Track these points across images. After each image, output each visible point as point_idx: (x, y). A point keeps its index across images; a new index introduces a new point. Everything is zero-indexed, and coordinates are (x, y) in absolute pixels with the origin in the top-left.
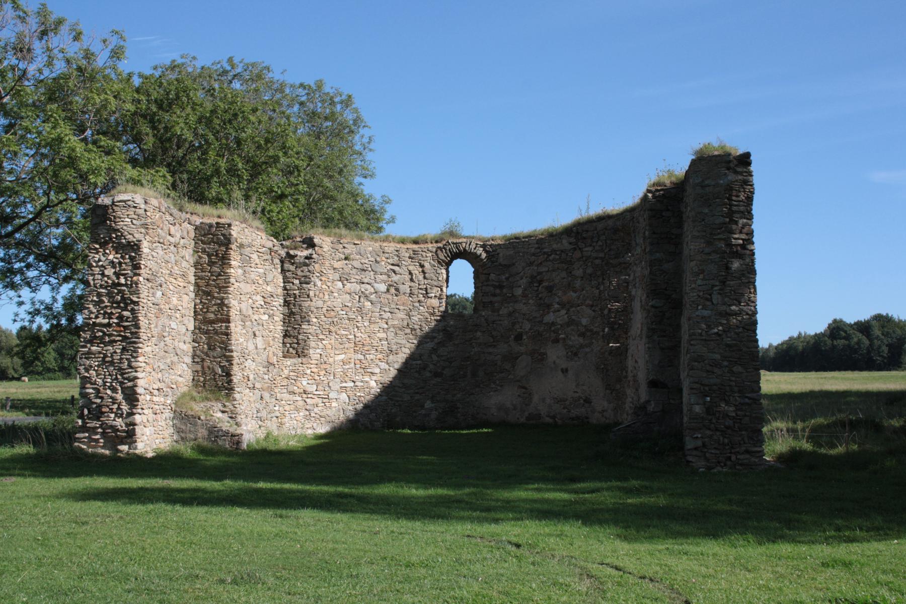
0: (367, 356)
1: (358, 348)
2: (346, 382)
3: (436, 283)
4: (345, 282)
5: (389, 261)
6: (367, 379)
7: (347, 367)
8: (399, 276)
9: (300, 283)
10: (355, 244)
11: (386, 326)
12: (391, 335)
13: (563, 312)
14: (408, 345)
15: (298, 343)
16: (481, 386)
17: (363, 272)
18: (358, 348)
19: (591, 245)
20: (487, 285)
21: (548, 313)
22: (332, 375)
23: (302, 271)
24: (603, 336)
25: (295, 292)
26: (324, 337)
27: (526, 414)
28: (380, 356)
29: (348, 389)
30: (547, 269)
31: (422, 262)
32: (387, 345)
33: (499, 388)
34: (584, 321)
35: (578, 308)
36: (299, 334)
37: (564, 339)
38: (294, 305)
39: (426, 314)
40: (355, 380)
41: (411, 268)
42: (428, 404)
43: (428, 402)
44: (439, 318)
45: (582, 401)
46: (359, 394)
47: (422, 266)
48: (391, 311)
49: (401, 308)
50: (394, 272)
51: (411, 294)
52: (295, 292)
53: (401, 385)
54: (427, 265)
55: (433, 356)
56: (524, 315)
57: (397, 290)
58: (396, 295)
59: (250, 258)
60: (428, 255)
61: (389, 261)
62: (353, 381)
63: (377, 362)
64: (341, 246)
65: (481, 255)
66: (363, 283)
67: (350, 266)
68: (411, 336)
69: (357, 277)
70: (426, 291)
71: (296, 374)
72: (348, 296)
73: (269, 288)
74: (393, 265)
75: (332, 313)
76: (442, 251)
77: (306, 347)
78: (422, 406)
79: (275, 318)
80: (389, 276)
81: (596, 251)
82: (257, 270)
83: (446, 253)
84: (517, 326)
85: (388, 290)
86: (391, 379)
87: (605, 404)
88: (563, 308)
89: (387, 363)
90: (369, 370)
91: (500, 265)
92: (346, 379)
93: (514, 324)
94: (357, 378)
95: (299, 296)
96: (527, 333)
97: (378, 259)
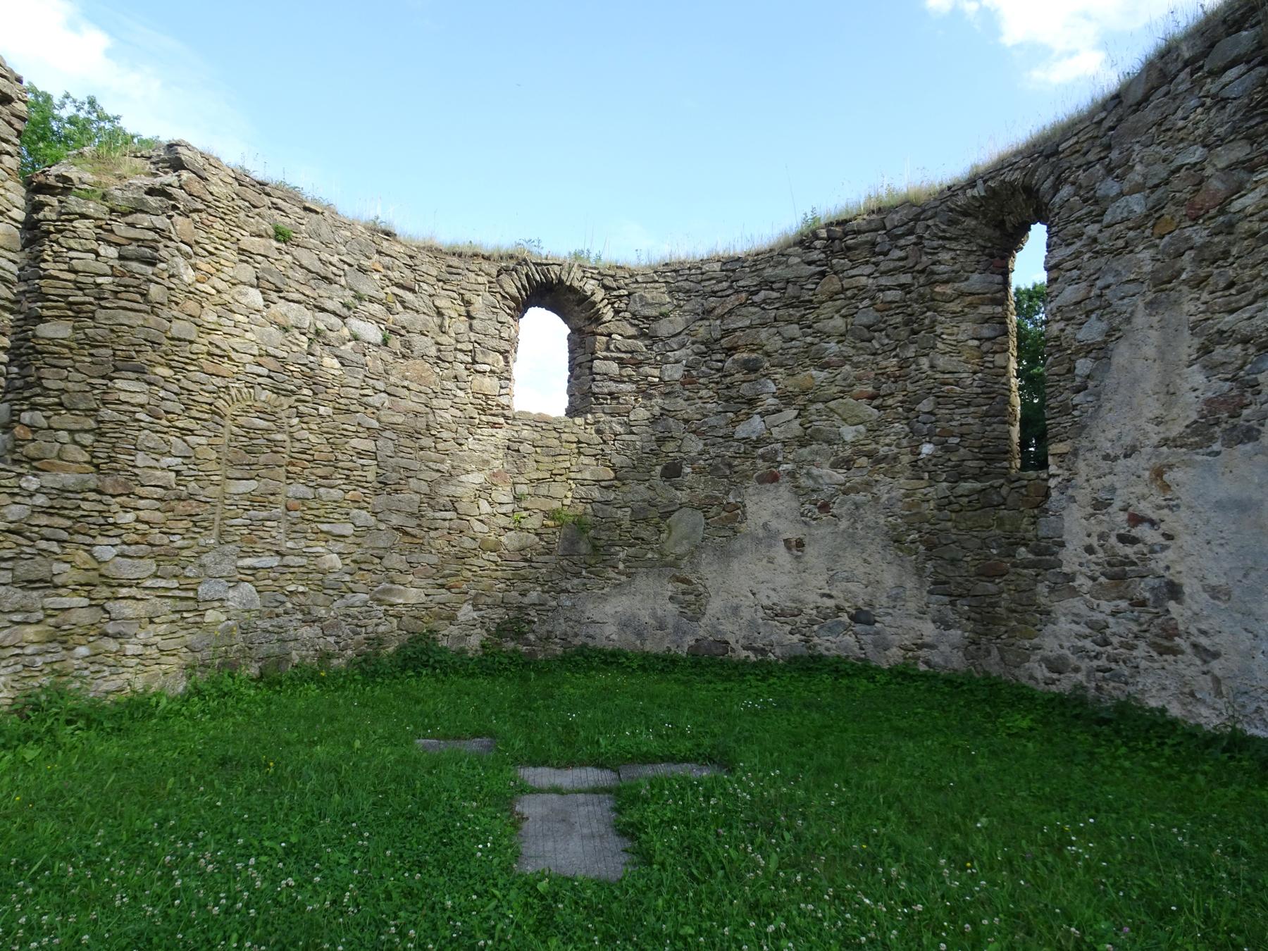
1: (297, 469)
2: (256, 554)
3: (494, 343)
4: (274, 296)
9: (121, 257)
13: (790, 413)
16: (584, 573)
17: (324, 285)
18: (297, 469)
19: (867, 263)
20: (605, 358)
21: (748, 416)
24: (914, 464)
25: (100, 280)
26: (192, 425)
27: (689, 640)
30: (748, 323)
31: (468, 296)
33: (623, 578)
34: (849, 433)
35: (832, 404)
37: (792, 474)
42: (466, 612)
43: (467, 608)
45: (845, 618)
48: (390, 389)
49: (413, 386)
50: (402, 302)
52: (100, 280)
53: (404, 567)
54: (478, 303)
56: (686, 421)
57: (408, 345)
64: (267, 200)
66: (323, 310)
71: (69, 523)
75: (227, 367)
78: (452, 619)
81: (883, 273)
84: (670, 446)
85: (385, 342)
87: (929, 629)
88: (788, 405)
89: (375, 514)
90: (325, 527)
91: (634, 316)
93: (661, 441)
94: (290, 544)
96: (693, 461)
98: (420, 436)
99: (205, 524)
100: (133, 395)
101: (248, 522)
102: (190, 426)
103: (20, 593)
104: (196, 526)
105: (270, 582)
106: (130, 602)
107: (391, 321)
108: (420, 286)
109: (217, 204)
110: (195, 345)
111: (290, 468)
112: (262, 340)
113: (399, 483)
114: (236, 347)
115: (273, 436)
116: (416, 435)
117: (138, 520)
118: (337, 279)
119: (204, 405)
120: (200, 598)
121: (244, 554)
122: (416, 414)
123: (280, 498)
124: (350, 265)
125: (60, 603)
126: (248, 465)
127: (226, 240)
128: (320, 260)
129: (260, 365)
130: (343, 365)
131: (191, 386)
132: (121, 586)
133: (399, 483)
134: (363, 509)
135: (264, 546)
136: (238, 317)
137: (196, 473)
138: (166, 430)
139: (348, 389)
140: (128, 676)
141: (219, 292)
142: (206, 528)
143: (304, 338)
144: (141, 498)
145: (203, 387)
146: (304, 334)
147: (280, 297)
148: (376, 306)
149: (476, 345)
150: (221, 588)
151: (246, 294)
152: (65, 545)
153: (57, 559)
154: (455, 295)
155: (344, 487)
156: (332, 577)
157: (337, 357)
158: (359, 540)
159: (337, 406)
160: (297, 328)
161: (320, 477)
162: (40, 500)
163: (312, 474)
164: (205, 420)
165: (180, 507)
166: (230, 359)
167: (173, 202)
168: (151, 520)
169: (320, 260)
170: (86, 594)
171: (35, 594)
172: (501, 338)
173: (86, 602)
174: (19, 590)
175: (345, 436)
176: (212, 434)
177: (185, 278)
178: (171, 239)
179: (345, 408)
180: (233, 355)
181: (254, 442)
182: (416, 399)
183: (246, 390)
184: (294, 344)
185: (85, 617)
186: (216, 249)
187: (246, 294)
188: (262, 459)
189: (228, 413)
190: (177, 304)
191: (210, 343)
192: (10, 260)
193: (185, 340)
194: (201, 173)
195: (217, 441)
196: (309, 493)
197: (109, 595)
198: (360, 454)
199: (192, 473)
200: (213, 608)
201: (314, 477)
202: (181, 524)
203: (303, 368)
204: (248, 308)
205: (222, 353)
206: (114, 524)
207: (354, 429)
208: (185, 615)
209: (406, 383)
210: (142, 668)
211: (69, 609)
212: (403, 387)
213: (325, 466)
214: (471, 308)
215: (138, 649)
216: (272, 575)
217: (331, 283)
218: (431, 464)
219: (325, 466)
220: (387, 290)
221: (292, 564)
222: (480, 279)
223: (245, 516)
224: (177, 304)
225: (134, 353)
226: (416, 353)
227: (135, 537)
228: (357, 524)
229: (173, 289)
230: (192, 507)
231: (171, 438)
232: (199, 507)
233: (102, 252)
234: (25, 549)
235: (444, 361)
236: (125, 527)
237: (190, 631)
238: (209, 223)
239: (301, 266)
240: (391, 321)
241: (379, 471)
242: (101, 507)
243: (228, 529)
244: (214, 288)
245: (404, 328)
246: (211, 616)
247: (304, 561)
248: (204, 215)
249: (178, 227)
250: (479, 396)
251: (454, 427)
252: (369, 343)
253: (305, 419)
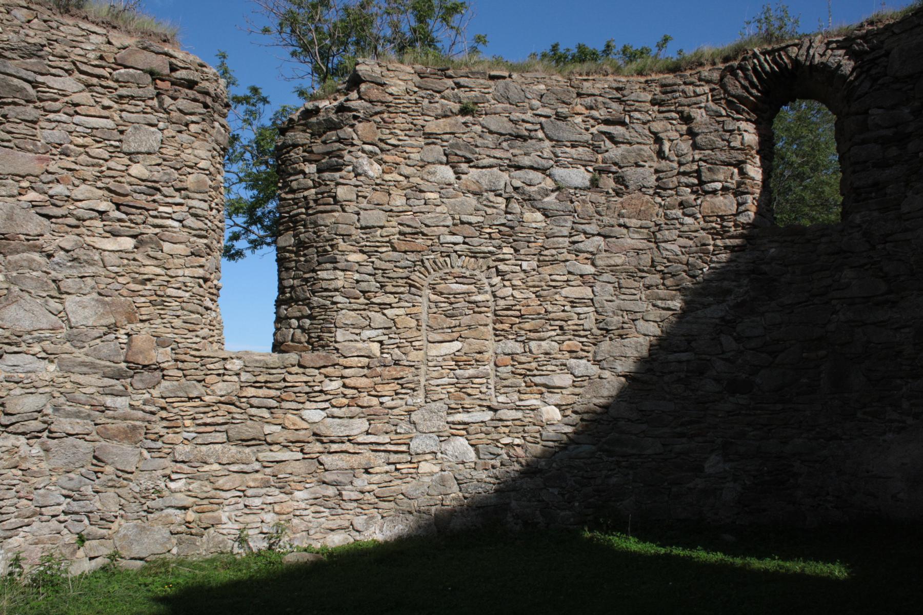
0: (533, 344)
2: (466, 410)
3: (723, 156)
4: (464, 166)
5: (595, 113)
6: (533, 401)
7: (471, 372)
8: (623, 146)
9: (319, 171)
10: (492, 78)
11: (590, 269)
12: (604, 291)
14: (655, 314)
15: (311, 317)
17: (518, 143)
18: (506, 326)
22: (421, 393)
23: (324, 142)
25: (306, 193)
26: (390, 299)
28: (575, 344)
29: (472, 428)
32: (593, 316)
36: (314, 292)
38: (305, 226)
39: (703, 234)
40: (494, 404)
41: (657, 126)
42: (713, 464)
44: (737, 241)
46: (507, 440)
47: (687, 119)
48: (606, 231)
49: (634, 222)
50: (611, 138)
51: (660, 188)
52: (306, 193)
54: (699, 115)
55: (723, 338)
57: (620, 180)
58: (618, 194)
59: (35, 84)
60: (698, 90)
61: (595, 113)
62: (490, 408)
63: (565, 358)
64: (450, 83)
65: (839, 66)
66: (519, 168)
67: (478, 128)
68: (662, 292)
69: (498, 153)
70: (699, 177)
71: (278, 393)
72: (472, 201)
73: (137, 170)
74: (607, 122)
75: (420, 241)
76: (736, 76)
77: (329, 325)
79: (167, 247)
80: (596, 149)
82: (77, 119)
83: (746, 77)
85: (594, 183)
86: (602, 401)
89: (597, 362)
90: (537, 380)
92: (467, 402)
94: (502, 399)
95: (316, 201)
97: (564, 110)
98: (644, 274)
99: (410, 385)
100: (330, 282)
101: (455, 380)
102: (387, 301)
103: (234, 449)
104: (403, 388)
105: (483, 435)
106: (342, 455)
107: (600, 160)
108: (630, 117)
109: (397, 101)
110: (384, 229)
111: (498, 326)
112: (455, 210)
113: (623, 328)
114: (427, 222)
115: (474, 298)
116: (640, 274)
117: (345, 386)
118: (533, 134)
119: (400, 281)
120: (412, 451)
121: (451, 410)
122: (638, 251)
123: (486, 355)
124: (549, 117)
125: (272, 457)
126: (450, 328)
127: (410, 130)
128: (511, 120)
129: (454, 234)
130: (547, 216)
131: (384, 265)
132: (332, 442)
133: (623, 328)
134: (582, 358)
135: (475, 401)
136: (429, 195)
137: (398, 341)
138: (363, 307)
139: (556, 239)
140: (348, 517)
141: (407, 177)
142: (414, 390)
143: (500, 199)
144: (346, 368)
145: (398, 264)
146: (500, 195)
147: (470, 167)
148: (580, 149)
149: (701, 163)
150: (432, 443)
151: (434, 173)
152: (273, 410)
153: (267, 422)
154: (674, 115)
155: (557, 338)
156: (550, 429)
157: (539, 209)
158: (577, 390)
159: (541, 258)
160: (491, 191)
161: (530, 331)
162: (244, 377)
163: (520, 328)
164: (402, 293)
165: (386, 372)
166: (424, 234)
167: (352, 114)
168: (358, 385)
169: (511, 120)
170: (299, 449)
171: (247, 450)
172: (733, 148)
173: (300, 456)
174: (234, 447)
175: (554, 287)
176: (410, 305)
177: (371, 173)
178: (353, 145)
179: (551, 258)
180: (425, 230)
181: (454, 306)
182: (636, 236)
183: (442, 259)
184: (489, 207)
185: (301, 468)
186: (399, 140)
187: (434, 173)
188: (465, 320)
189: (425, 283)
190: (365, 197)
191: (399, 224)
192: (201, 200)
193: (374, 227)
194: (379, 81)
195: (414, 310)
196: (518, 348)
197: (321, 450)
198: (573, 303)
199: (392, 341)
200: (426, 460)
201: (523, 332)
202: (387, 387)
203: (502, 228)
204: (439, 184)
205: (414, 231)
206: (321, 391)
207: (565, 278)
208: (398, 466)
209: (621, 221)
210: (360, 510)
211: (285, 461)
212: (620, 225)
213: (533, 319)
214: (692, 125)
215: (355, 495)
216: (484, 429)
217: (525, 140)
218: (659, 303)
219: (533, 319)
220: (594, 130)
221: (504, 418)
222: (698, 90)
223: (452, 375)
224: (365, 197)
225: (329, 248)
226: (631, 187)
227: (346, 401)
228: (576, 374)
229: (361, 186)
230: (395, 372)
231: (369, 313)
232: (403, 371)
233: (307, 171)
234: (236, 416)
235: (665, 189)
236: (332, 392)
237: (404, 480)
238: (391, 120)
239: (491, 132)
240: (600, 160)
241: (600, 317)
242: (305, 379)
243: (433, 388)
244: (401, 175)
245: (615, 164)
246: (425, 467)
247: (519, 415)
248: (385, 115)
249: (359, 133)
250: (711, 219)
251: (684, 258)
252: (576, 188)
253: (507, 277)
